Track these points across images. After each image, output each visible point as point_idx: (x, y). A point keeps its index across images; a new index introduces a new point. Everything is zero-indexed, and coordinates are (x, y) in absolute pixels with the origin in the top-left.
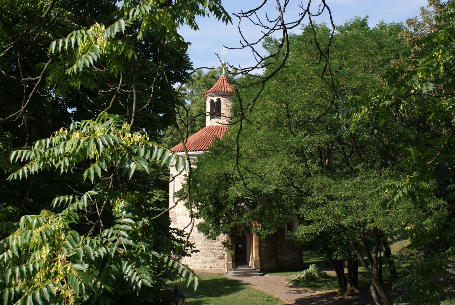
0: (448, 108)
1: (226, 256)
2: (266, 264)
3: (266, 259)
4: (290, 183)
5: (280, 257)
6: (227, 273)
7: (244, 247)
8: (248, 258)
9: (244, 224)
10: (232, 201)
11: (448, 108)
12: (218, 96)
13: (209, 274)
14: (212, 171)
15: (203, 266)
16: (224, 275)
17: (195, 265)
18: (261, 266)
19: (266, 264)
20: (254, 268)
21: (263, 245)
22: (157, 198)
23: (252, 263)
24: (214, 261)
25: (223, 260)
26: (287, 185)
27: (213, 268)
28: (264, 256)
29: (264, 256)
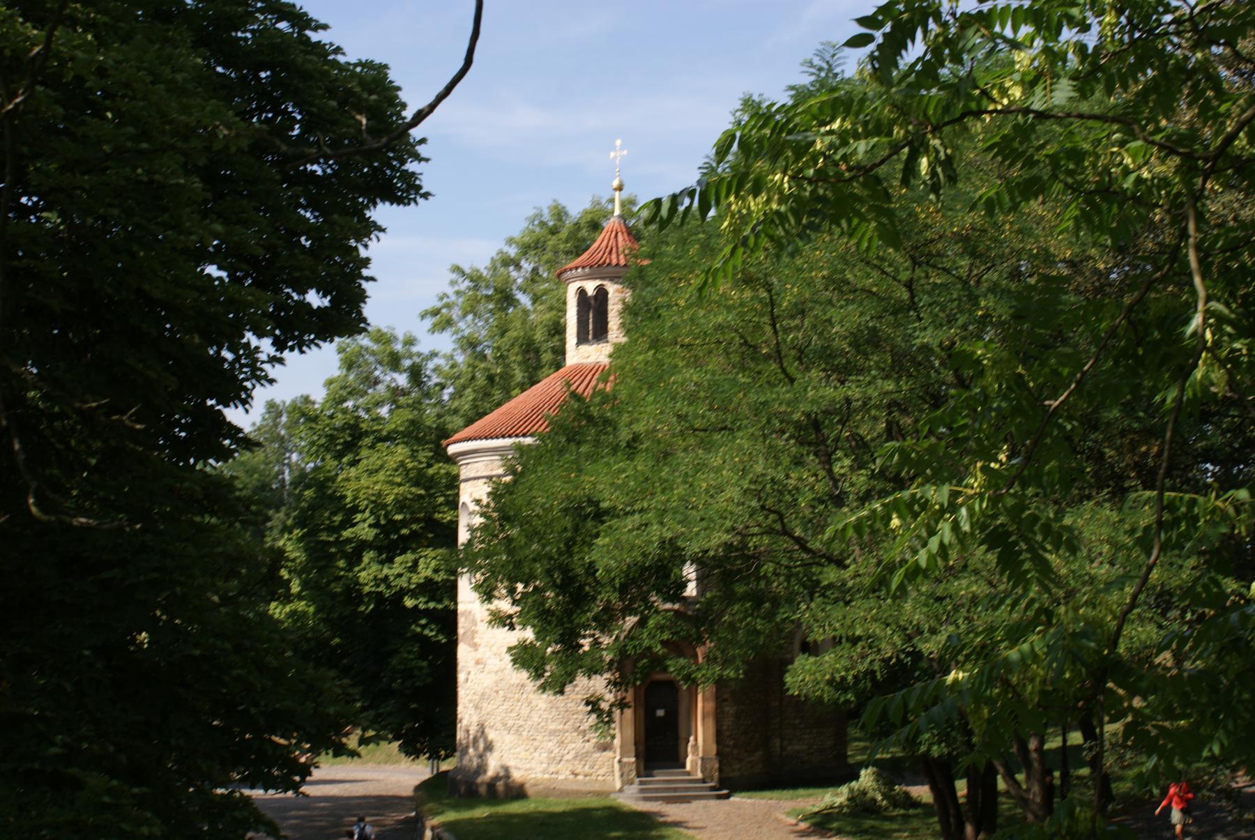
0: (1132, 177)
1: (617, 742)
2: (737, 767)
3: (735, 751)
4: (778, 527)
5: (778, 744)
6: (621, 790)
7: (673, 715)
8: (682, 748)
9: (649, 648)
10: (614, 579)
11: (1132, 177)
12: (602, 278)
13: (568, 793)
14: (552, 492)
15: (552, 769)
16: (612, 796)
17: (528, 766)
18: (721, 770)
19: (737, 767)
20: (700, 775)
21: (727, 709)
22: (429, 573)
23: (694, 763)
24: (581, 757)
25: (608, 754)
26: (769, 531)
27: (580, 777)
29: (731, 743)
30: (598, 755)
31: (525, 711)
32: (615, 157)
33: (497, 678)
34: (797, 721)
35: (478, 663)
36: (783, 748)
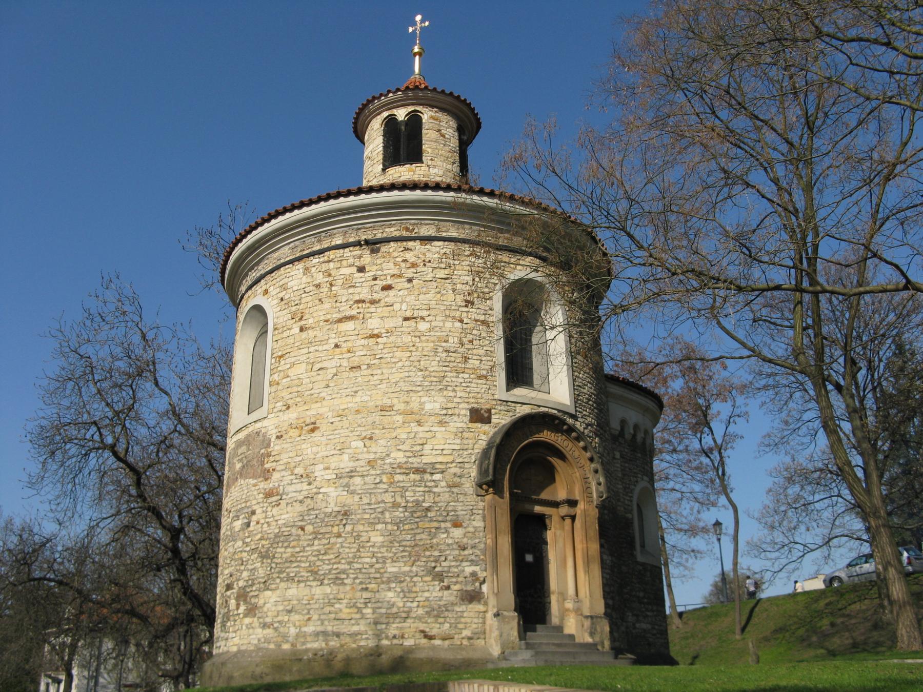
12: (413, 104)
27: (437, 642)
30: (463, 608)
31: (348, 552)
32: (414, 31)
33: (304, 508)
34: (641, 594)
36: (634, 624)
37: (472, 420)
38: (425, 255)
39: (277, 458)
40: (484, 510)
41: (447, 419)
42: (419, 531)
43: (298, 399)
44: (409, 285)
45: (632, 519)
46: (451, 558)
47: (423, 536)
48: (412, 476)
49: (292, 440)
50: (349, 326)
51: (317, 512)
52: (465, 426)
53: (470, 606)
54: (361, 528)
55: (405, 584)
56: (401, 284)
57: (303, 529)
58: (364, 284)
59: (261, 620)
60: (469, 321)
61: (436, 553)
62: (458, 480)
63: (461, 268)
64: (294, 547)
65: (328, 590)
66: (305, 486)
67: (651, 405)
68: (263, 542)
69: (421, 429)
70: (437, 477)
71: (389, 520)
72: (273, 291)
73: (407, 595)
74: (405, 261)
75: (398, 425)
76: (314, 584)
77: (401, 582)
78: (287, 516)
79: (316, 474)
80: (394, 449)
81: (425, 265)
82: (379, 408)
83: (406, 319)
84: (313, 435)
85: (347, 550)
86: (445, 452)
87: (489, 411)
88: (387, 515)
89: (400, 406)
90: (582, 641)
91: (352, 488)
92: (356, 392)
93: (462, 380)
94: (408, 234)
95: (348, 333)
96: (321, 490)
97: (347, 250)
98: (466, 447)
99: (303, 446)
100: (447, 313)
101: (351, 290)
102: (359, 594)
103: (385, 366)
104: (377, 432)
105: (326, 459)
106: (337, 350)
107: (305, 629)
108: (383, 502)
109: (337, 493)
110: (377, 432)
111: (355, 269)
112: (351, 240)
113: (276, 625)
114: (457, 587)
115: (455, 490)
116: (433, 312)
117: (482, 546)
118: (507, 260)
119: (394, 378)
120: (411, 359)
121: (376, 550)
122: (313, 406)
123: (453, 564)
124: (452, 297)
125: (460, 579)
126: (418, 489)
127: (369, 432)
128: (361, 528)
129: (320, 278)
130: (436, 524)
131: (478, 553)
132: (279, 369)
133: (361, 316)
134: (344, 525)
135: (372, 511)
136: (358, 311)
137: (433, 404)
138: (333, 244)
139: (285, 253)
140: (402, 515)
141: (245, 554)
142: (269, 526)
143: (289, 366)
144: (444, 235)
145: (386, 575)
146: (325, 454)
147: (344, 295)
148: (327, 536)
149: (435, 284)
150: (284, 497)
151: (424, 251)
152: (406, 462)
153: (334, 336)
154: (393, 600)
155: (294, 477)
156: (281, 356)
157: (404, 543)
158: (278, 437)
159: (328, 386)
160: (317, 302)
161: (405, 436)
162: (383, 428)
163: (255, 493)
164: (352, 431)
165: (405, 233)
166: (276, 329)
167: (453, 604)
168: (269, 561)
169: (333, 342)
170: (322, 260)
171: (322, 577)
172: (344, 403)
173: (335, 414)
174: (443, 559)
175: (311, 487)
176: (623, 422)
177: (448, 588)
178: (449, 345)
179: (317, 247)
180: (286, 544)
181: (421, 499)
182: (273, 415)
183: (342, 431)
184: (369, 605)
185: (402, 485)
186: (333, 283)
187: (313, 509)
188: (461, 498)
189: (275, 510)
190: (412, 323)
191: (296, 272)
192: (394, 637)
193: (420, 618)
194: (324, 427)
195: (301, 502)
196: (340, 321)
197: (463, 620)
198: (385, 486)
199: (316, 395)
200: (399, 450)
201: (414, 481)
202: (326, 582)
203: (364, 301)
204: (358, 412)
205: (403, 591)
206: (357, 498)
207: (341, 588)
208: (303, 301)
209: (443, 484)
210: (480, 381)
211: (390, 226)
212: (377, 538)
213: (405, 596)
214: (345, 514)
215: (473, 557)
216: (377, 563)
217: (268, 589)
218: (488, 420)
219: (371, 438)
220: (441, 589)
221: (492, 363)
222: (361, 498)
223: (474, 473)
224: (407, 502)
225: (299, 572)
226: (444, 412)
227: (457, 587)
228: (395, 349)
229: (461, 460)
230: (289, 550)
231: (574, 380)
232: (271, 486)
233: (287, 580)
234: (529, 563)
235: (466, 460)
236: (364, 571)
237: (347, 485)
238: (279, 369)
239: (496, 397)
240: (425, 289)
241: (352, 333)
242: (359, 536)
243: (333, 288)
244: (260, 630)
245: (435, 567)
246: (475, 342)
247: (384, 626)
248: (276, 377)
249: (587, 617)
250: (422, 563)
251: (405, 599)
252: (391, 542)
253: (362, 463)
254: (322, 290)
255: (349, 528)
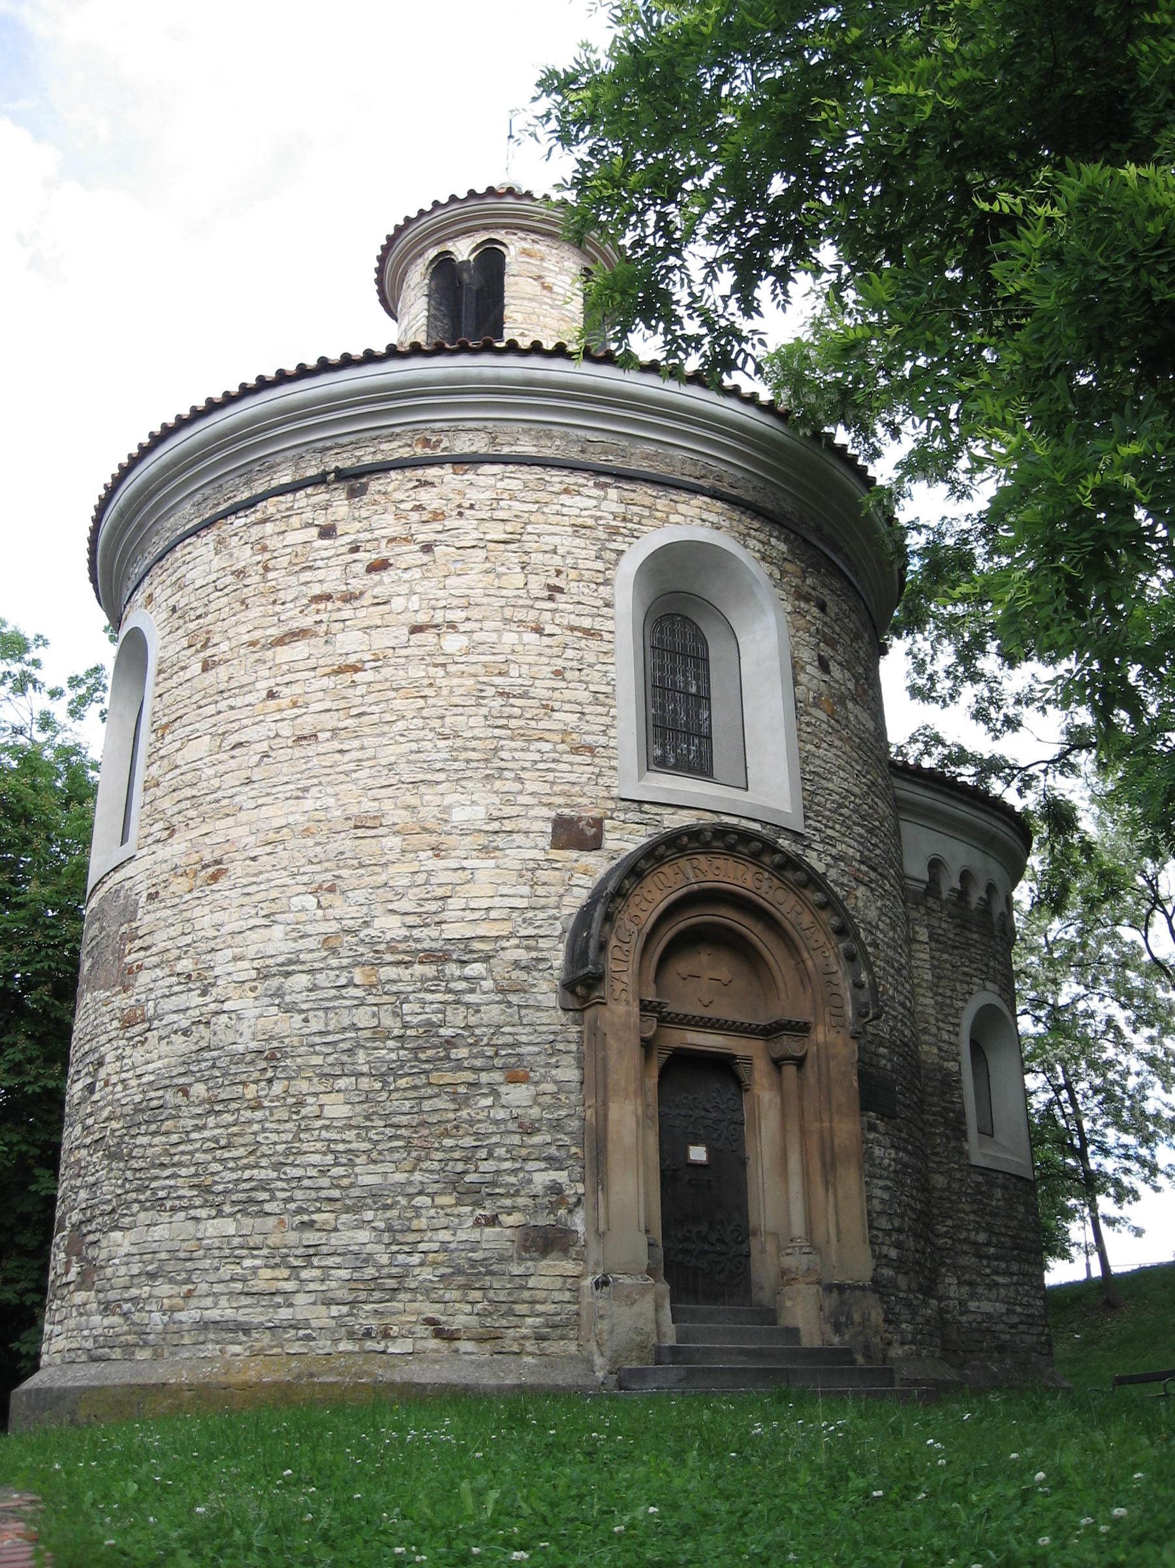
12: (486, 228)
15: (365, 1319)
17: (285, 1313)
21: (878, 1152)
24: (468, 1273)
28: (893, 1253)
31: (276, 1139)
34: (982, 1237)
35: (127, 1023)
36: (962, 1303)
37: (555, 845)
38: (462, 493)
39: (148, 940)
40: (580, 1043)
41: (500, 841)
42: (430, 1091)
43: (191, 813)
44: (426, 558)
45: (959, 1073)
46: (500, 1152)
47: (439, 1103)
48: (418, 969)
49: (177, 900)
50: (300, 649)
51: (215, 1054)
52: (540, 855)
53: (544, 1263)
54: (304, 1086)
55: (394, 1213)
56: (411, 556)
57: (186, 1094)
58: (332, 562)
59: (101, 1295)
60: (557, 630)
61: (469, 1142)
62: (523, 975)
63: (541, 518)
64: (167, 1133)
65: (229, 1227)
66: (195, 999)
67: (1002, 831)
68: (114, 1125)
69: (443, 863)
70: (476, 969)
71: (365, 1069)
72: (161, 594)
73: (399, 1237)
74: (419, 508)
75: (391, 857)
76: (203, 1213)
77: (387, 1207)
78: (159, 1064)
79: (218, 971)
80: (378, 909)
81: (460, 514)
82: (352, 823)
83: (416, 629)
84: (215, 887)
85: (274, 1137)
86: (493, 914)
87: (598, 823)
88: (361, 1056)
89: (400, 817)
90: (817, 1343)
91: (288, 999)
92: (306, 790)
93: (537, 757)
94: (429, 451)
95: (297, 666)
96: (227, 1006)
97: (302, 493)
98: (543, 901)
99: (197, 912)
100: (508, 612)
101: (306, 576)
102: (292, 1237)
103: (368, 730)
104: (344, 873)
105: (239, 939)
106: (272, 704)
107: (179, 1316)
108: (354, 1027)
109: (257, 1011)
110: (344, 873)
111: (315, 531)
112: (311, 472)
113: (126, 1307)
114: (515, 1219)
115: (514, 999)
116: (474, 613)
117: (575, 1124)
118: (648, 501)
119: (388, 755)
120: (425, 713)
121: (334, 1136)
122: (220, 824)
123: (507, 1165)
124: (519, 580)
125: (521, 1201)
126: (429, 997)
127: (328, 876)
128: (304, 1086)
129: (245, 556)
130: (470, 1077)
131: (567, 1140)
132: (161, 753)
133: (324, 627)
134: (270, 1081)
135: (329, 1050)
136: (318, 618)
137: (470, 808)
138: (274, 484)
139: (186, 515)
140: (393, 1056)
141: (84, 1152)
142: (125, 1089)
143: (178, 744)
144: (506, 450)
145: (355, 1192)
146: (235, 927)
147: (290, 586)
148: (234, 1106)
149: (482, 554)
150: (156, 1024)
151: (460, 486)
152: (406, 939)
153: (267, 673)
154: (369, 1248)
155: (174, 979)
156: (166, 726)
157: (396, 1120)
158: (152, 897)
159: (249, 781)
160: (237, 606)
161: (405, 881)
162: (361, 866)
163: (106, 1019)
164: (294, 875)
165: (420, 451)
166: (160, 672)
167: (502, 1259)
168: (122, 1165)
169: (263, 685)
170: (252, 518)
171: (219, 1199)
172: (277, 814)
173: (262, 837)
174: (483, 1154)
175: (208, 999)
176: (935, 865)
177: (493, 1221)
178: (508, 681)
179: (245, 495)
180: (153, 1127)
181: (435, 1018)
182: (145, 851)
183: (275, 874)
184: (315, 1261)
185: (394, 988)
186: (271, 564)
187: (208, 1048)
188: (530, 1016)
189: (138, 1055)
190: (428, 637)
191: (203, 550)
192: (368, 1334)
193: (427, 1291)
194: (238, 869)
195: (186, 1032)
196: (280, 641)
197: (526, 1294)
198: (359, 993)
199: (225, 802)
200: (392, 911)
201: (424, 979)
202: (227, 1209)
203: (328, 597)
204: (307, 833)
205: (390, 1229)
206: (299, 1018)
207: (259, 1220)
208: (213, 607)
209: (488, 984)
210: (578, 759)
211: (393, 437)
212: (337, 1109)
213: (395, 1242)
214: (272, 1057)
215: (553, 1151)
216: (336, 1164)
217: (117, 1228)
218: (593, 843)
219: (331, 890)
220: (477, 1224)
221: (608, 720)
222: (306, 1020)
223: (559, 959)
224: (406, 1026)
225: (175, 1188)
226: (496, 826)
227: (515, 1219)
228: (392, 694)
229: (531, 931)
230: (156, 1140)
231: (805, 761)
232: (132, 1002)
233: (152, 1208)
234: (697, 1166)
235: (541, 932)
236: (306, 1183)
237: (279, 993)
238: (161, 753)
239: (615, 792)
240: (459, 565)
241: (301, 665)
242: (301, 1104)
243: (270, 575)
244: (96, 1319)
245: (465, 1172)
246: (568, 675)
247: (345, 1309)
248: (154, 770)
249: (829, 1288)
250: (436, 1166)
251: (394, 1248)
252: (368, 1118)
253: (311, 943)
254: (246, 582)
255: (278, 1088)
